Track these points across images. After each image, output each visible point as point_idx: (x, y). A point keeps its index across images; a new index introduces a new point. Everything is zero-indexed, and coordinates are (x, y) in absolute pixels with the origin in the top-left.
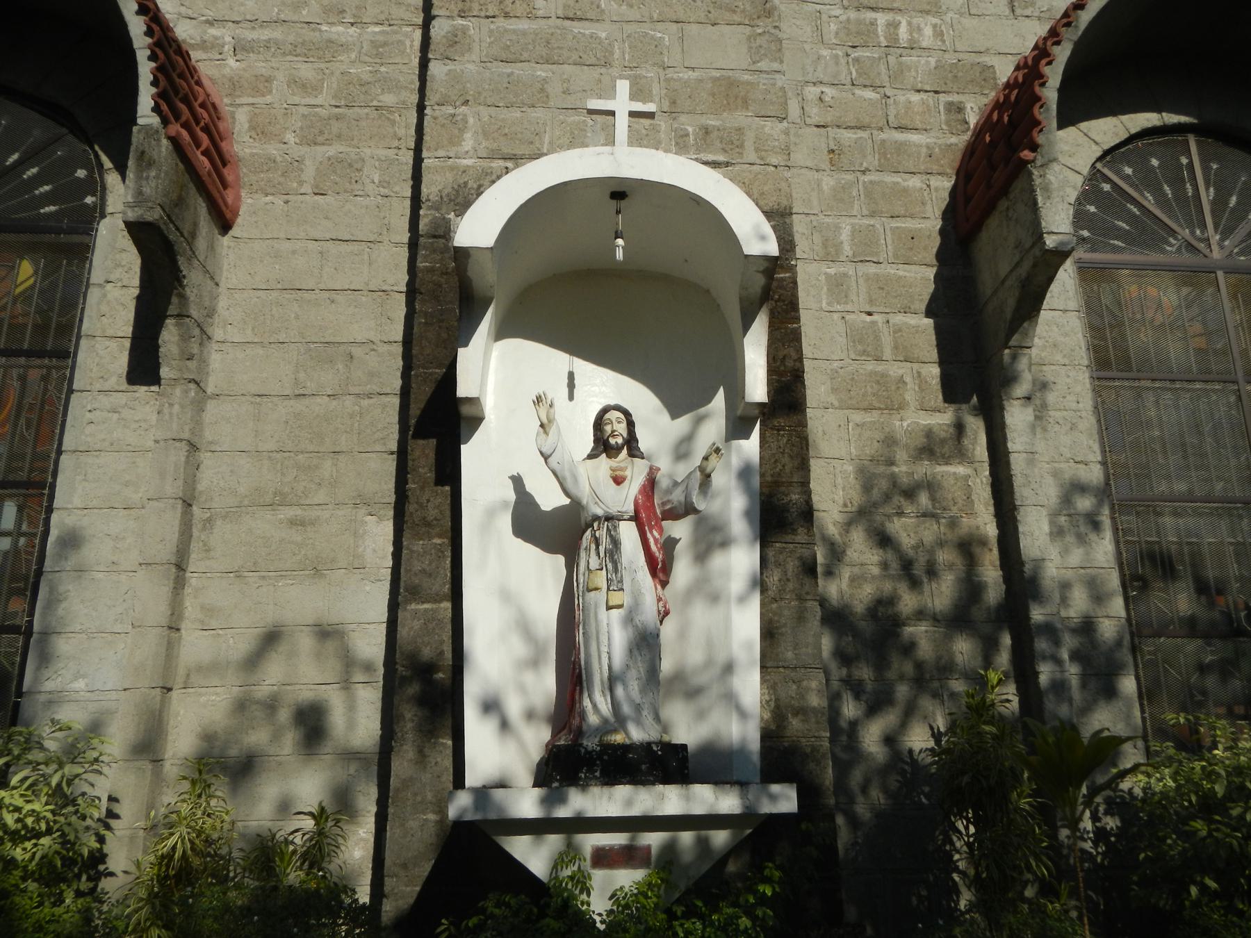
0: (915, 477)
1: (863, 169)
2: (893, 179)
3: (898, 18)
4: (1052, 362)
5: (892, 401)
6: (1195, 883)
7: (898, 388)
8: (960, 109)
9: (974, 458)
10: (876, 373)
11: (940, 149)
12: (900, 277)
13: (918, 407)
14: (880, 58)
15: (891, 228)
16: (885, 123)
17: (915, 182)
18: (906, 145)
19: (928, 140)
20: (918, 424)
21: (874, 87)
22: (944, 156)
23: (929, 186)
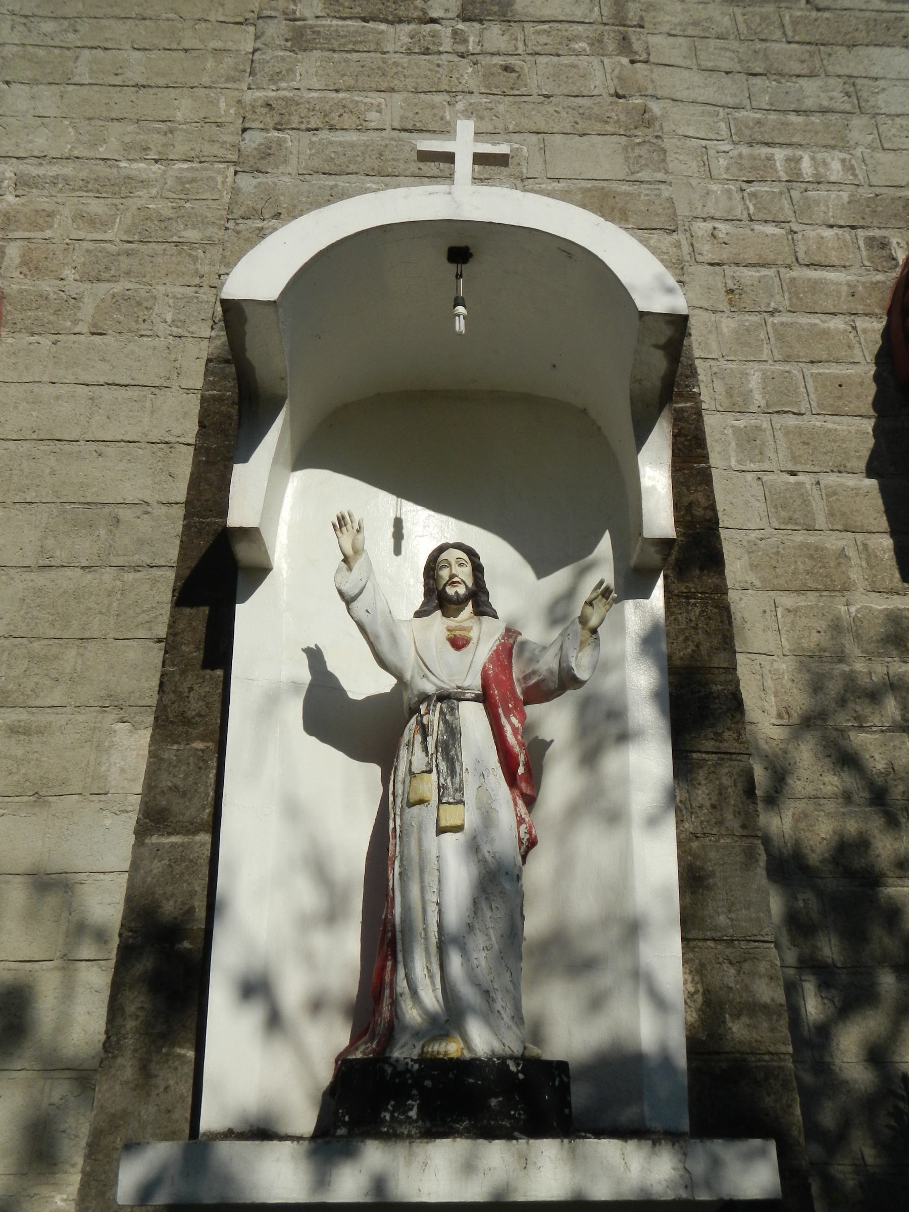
0: (874, 678)
1: (771, 309)
2: (809, 321)
3: (799, 153)
5: (832, 581)
7: (839, 563)
8: (884, 245)
10: (808, 546)
11: (865, 287)
12: (829, 430)
13: (869, 588)
14: (781, 193)
15: (812, 374)
16: (794, 260)
17: (837, 324)
18: (822, 283)
19: (849, 278)
20: (870, 609)
21: (777, 223)
22: (871, 295)
23: (854, 328)
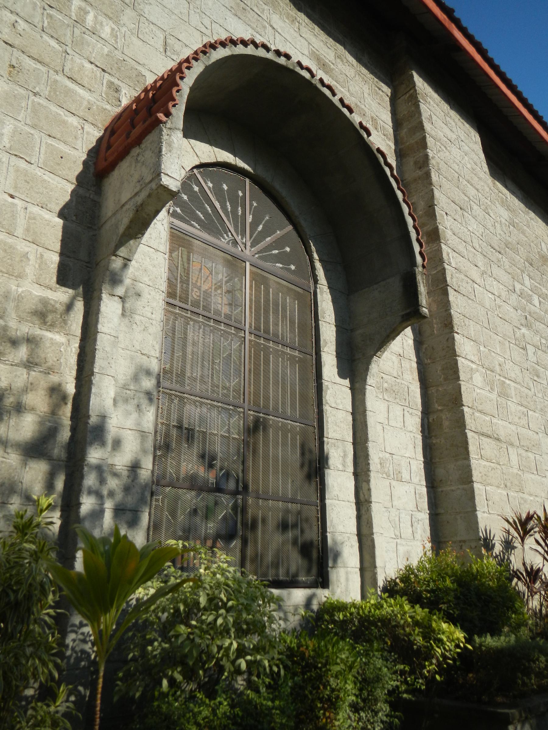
0: (18, 333)
1: (35, 91)
2: (57, 111)
3: (89, 8)
4: (141, 281)
5: (13, 269)
6: (166, 676)
7: (22, 261)
8: (117, 90)
9: (70, 331)
10: (5, 244)
11: (97, 108)
12: (45, 181)
13: (35, 281)
14: (68, 26)
15: (46, 143)
16: (61, 70)
17: (73, 121)
18: (73, 92)
19: (90, 98)
20: (31, 293)
21: (59, 42)
22: (99, 114)
23: (83, 128)
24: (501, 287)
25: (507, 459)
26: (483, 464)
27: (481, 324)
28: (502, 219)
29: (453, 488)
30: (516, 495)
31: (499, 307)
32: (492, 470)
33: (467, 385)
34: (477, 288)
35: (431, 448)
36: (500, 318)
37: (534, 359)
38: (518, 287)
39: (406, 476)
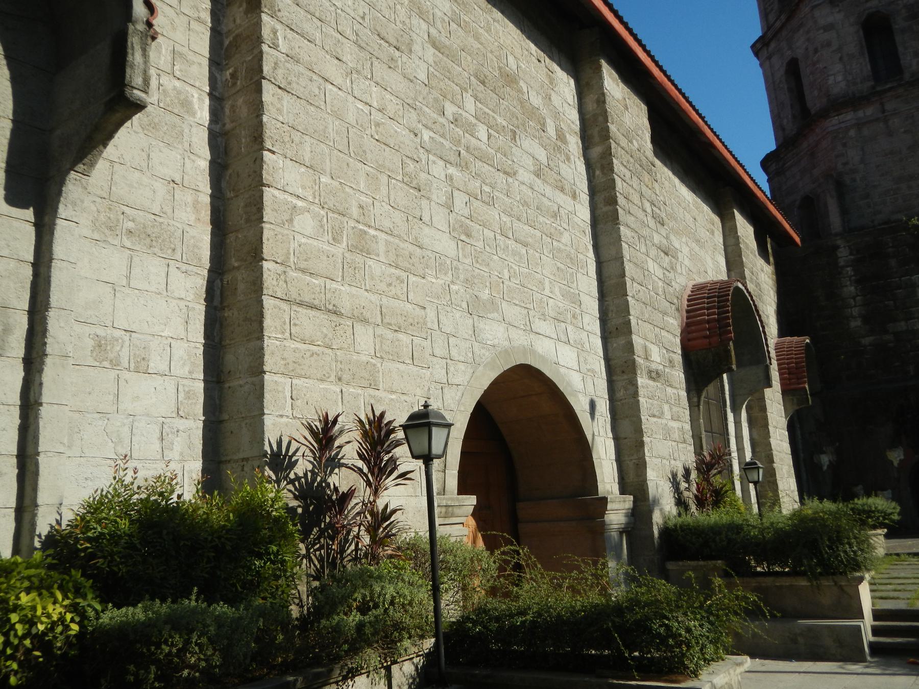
24: (388, 96)
25: (350, 341)
26: (293, 346)
27: (331, 144)
28: (436, 10)
29: (241, 382)
30: (360, 391)
31: (378, 125)
32: (312, 355)
33: (278, 229)
34: (331, 90)
35: (221, 325)
36: (377, 140)
37: (466, 212)
38: (450, 109)
39: (157, 363)
